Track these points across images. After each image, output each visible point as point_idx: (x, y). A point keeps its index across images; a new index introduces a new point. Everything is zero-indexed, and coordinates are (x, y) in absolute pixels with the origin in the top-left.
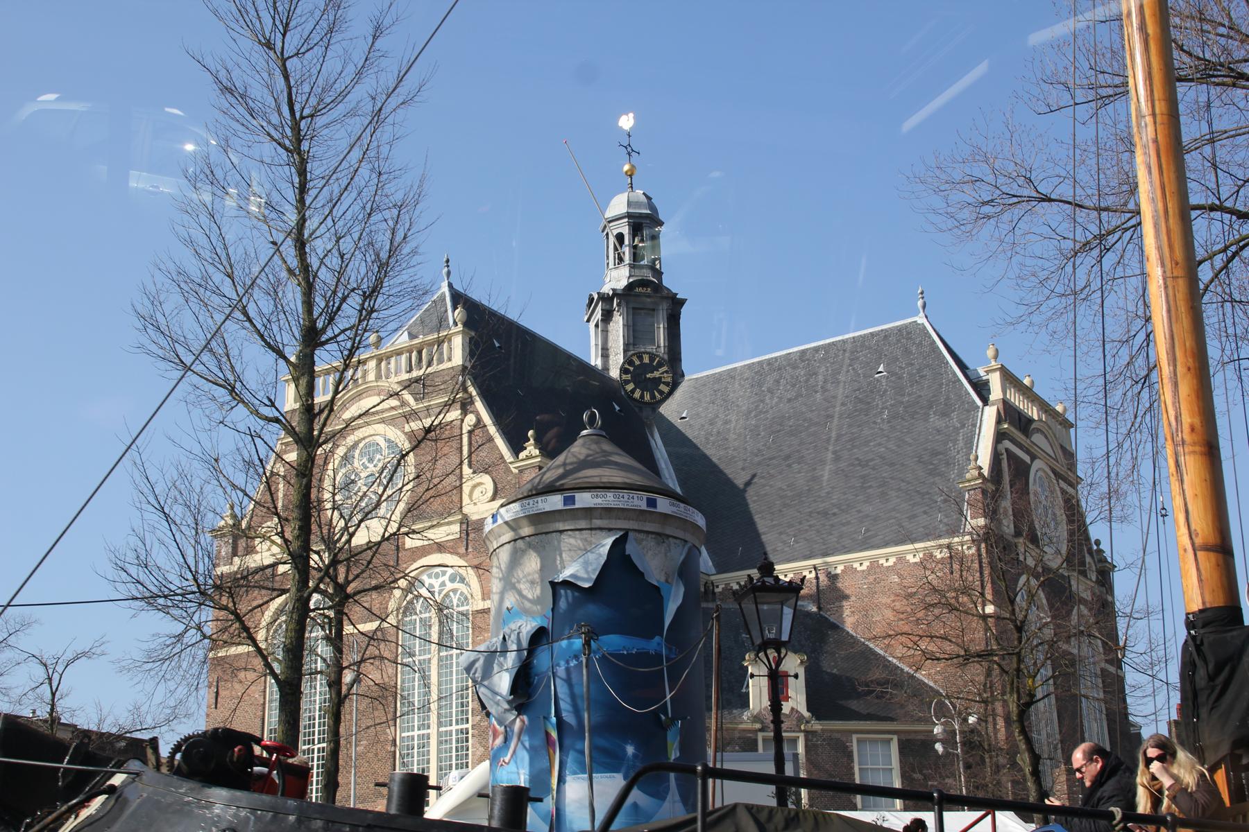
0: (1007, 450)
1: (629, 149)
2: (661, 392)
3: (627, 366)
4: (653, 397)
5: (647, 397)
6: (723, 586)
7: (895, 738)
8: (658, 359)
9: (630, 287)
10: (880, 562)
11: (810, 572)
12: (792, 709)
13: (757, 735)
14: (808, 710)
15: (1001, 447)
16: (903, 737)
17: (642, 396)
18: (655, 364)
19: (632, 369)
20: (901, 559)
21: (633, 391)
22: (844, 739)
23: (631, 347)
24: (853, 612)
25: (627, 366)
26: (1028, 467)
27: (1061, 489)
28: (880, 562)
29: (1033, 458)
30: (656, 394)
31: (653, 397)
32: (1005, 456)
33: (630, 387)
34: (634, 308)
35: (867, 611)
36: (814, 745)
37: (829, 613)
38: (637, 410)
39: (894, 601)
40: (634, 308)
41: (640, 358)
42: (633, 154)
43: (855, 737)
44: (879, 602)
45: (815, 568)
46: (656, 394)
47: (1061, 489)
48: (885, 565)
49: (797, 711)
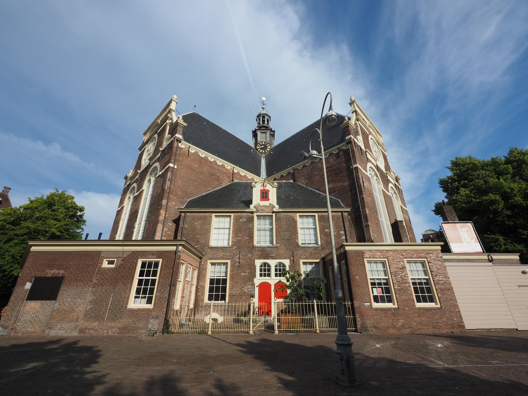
4: (265, 151)
5: (263, 151)
11: (292, 171)
12: (270, 204)
14: (277, 204)
17: (262, 151)
22: (293, 216)
31: (265, 151)
36: (279, 218)
38: (261, 155)
39: (319, 173)
41: (262, 143)
43: (298, 214)
44: (315, 174)
45: (294, 169)
49: (272, 205)
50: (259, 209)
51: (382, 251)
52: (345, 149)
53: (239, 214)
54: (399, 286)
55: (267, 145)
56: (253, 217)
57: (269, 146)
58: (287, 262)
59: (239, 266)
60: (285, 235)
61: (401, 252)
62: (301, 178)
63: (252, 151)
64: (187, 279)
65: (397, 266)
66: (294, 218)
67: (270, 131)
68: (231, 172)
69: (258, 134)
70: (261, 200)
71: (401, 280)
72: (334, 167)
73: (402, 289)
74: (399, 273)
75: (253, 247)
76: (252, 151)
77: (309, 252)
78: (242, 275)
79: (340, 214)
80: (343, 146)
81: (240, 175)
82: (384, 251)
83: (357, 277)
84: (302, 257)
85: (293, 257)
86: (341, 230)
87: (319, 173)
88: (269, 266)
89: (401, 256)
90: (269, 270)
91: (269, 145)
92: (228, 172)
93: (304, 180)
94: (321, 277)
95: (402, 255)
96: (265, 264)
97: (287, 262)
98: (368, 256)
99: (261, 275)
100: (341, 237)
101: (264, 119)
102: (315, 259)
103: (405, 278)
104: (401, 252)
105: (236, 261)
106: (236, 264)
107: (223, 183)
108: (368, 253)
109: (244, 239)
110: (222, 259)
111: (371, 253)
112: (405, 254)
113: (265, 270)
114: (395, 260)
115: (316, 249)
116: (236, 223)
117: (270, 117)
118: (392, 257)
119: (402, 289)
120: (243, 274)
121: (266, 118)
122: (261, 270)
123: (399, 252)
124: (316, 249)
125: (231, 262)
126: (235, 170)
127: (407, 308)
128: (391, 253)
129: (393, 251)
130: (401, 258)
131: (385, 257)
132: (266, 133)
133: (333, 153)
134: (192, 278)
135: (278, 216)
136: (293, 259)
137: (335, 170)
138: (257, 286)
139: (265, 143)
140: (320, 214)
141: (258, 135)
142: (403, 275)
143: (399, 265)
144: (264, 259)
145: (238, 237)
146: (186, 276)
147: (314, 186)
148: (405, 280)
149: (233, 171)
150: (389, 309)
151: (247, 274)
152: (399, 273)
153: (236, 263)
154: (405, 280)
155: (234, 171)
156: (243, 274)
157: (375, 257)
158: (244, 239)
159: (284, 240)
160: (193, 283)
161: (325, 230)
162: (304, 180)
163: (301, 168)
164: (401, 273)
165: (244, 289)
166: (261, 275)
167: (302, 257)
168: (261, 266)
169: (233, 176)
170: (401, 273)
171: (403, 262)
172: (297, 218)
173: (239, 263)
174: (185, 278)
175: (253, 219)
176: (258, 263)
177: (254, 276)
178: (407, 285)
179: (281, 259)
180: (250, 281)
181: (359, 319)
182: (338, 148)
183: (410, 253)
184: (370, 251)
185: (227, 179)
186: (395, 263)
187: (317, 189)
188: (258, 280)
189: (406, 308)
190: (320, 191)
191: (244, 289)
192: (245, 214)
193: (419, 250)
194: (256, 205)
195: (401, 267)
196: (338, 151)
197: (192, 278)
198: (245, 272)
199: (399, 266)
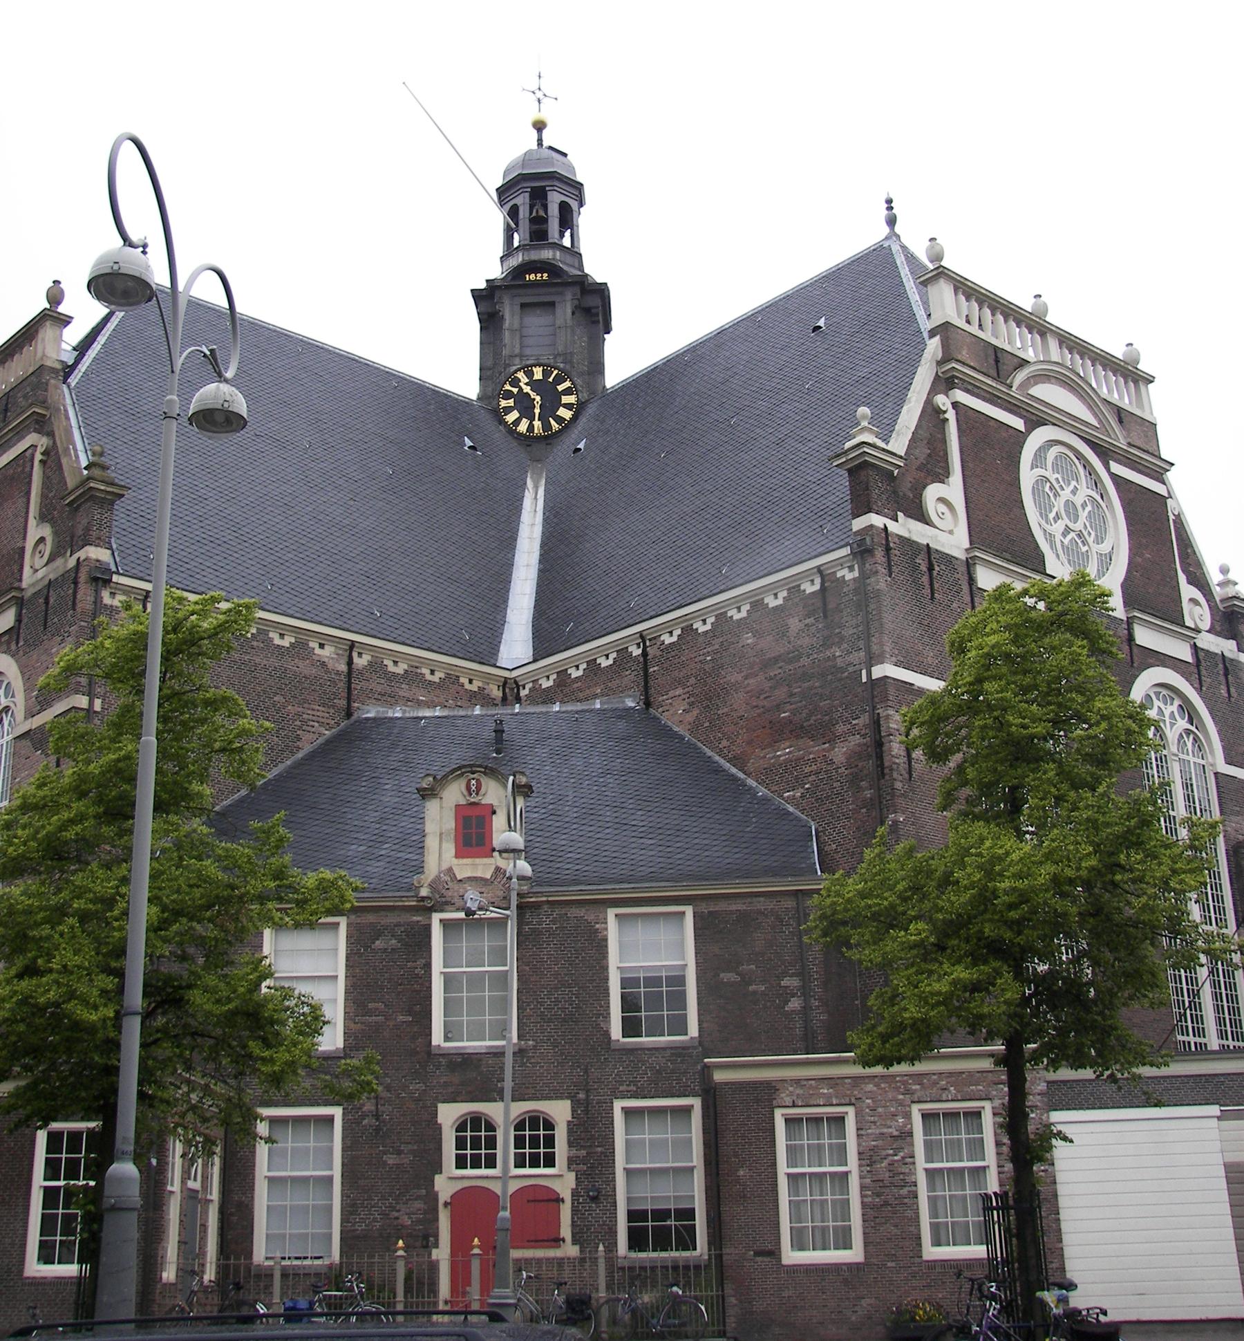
0: (955, 405)
1: (539, 94)
2: (560, 420)
3: (508, 387)
6: (531, 685)
7: (689, 911)
8: (556, 372)
9: (517, 273)
10: (729, 615)
11: (638, 645)
13: (430, 918)
15: (941, 400)
16: (704, 908)
18: (551, 380)
19: (515, 390)
20: (757, 604)
21: (517, 422)
23: (517, 361)
24: (693, 703)
25: (508, 387)
26: (1019, 439)
27: (1115, 478)
28: (729, 614)
29: (1035, 421)
30: (553, 422)
31: (547, 426)
32: (951, 415)
33: (514, 416)
34: (523, 306)
35: (710, 699)
36: (534, 930)
37: (660, 710)
40: (523, 306)
42: (544, 100)
43: (611, 913)
45: (642, 637)
46: (553, 422)
47: (1115, 478)
48: (737, 617)
50: (450, 893)
51: (838, 1081)
52: (847, 578)
53: (371, 918)
54: (878, 1195)
55: (560, 388)
56: (427, 929)
57: (568, 392)
58: (560, 1111)
59: (378, 1129)
60: (557, 1001)
61: (904, 1083)
62: (671, 694)
63: (468, 442)
64: (191, 1184)
65: (885, 1130)
66: (597, 926)
67: (577, 290)
68: (338, 673)
69: (507, 316)
70: (458, 855)
71: (887, 1174)
72: (805, 661)
73: (886, 1204)
74: (884, 1153)
75: (429, 1053)
76: (468, 442)
77: (652, 1068)
78: (390, 1162)
79: (790, 903)
80: (839, 563)
81: (386, 673)
82: (846, 1081)
83: (741, 1173)
84: (621, 1088)
85: (588, 1091)
86: (785, 974)
87: (746, 678)
88: (491, 1127)
89: (901, 1097)
90: (491, 1143)
91: (567, 384)
92: (327, 672)
93: (687, 707)
94: (695, 1163)
95: (908, 1092)
96: (476, 1121)
97: (560, 1111)
98: (788, 1101)
99: (461, 1162)
100: (786, 1002)
101: (542, 213)
102: (673, 1096)
103: (905, 1169)
104: (904, 1083)
105: (365, 1109)
106: (365, 1122)
107: (306, 737)
108: (791, 1089)
109: (391, 1023)
110: (312, 1105)
111: (799, 1091)
112: (918, 1087)
113: (476, 1143)
114: (880, 1110)
115: (679, 1055)
116: (361, 955)
117: (578, 187)
118: (869, 1101)
119: (886, 1204)
120: (391, 1160)
121: (554, 199)
122: (460, 1143)
123: (900, 1081)
124: (679, 1055)
125: (344, 1114)
126: (360, 654)
127: (893, 1264)
128: (870, 1087)
129: (876, 1080)
130: (901, 1104)
131: (847, 1101)
132: (552, 305)
133: (802, 588)
134: (205, 1178)
135: (528, 924)
136: (588, 1096)
137: (805, 677)
138: (446, 1204)
139: (546, 374)
140: (704, 908)
141: (507, 324)
142: (896, 1158)
143: (890, 1127)
144: (472, 1101)
145: (369, 1013)
146: (186, 1175)
147: (725, 743)
148: (901, 1177)
149: (350, 662)
150: (836, 1268)
151: (406, 1160)
152: (884, 1153)
153: (364, 1116)
154: (901, 1177)
155: (356, 659)
156: (391, 1160)
157: (812, 1103)
158: (391, 1023)
159: (550, 1021)
160: (209, 1197)
161: (722, 975)
162: (687, 707)
163: (674, 639)
164: (891, 1152)
165: (396, 1214)
166: (461, 1162)
167: (621, 1088)
168: (461, 1127)
169: (349, 688)
170: (891, 1152)
171: (908, 1116)
172: (606, 929)
173: (377, 1116)
174: (183, 1182)
175: (429, 936)
176: (449, 1114)
177: (438, 1169)
178: (904, 1191)
179: (538, 1099)
180: (418, 1187)
181: (733, 1300)
182: (819, 570)
183: (936, 1083)
184: (797, 1082)
185: (321, 712)
186: (876, 1119)
187: (733, 761)
188: (446, 1184)
189: (889, 1264)
190: (745, 773)
191: (396, 1214)
192: (391, 919)
193: (970, 1073)
194: (438, 877)
195: (896, 1133)
196: (822, 584)
197: (205, 1178)
198: (399, 1152)
199: (890, 1130)
